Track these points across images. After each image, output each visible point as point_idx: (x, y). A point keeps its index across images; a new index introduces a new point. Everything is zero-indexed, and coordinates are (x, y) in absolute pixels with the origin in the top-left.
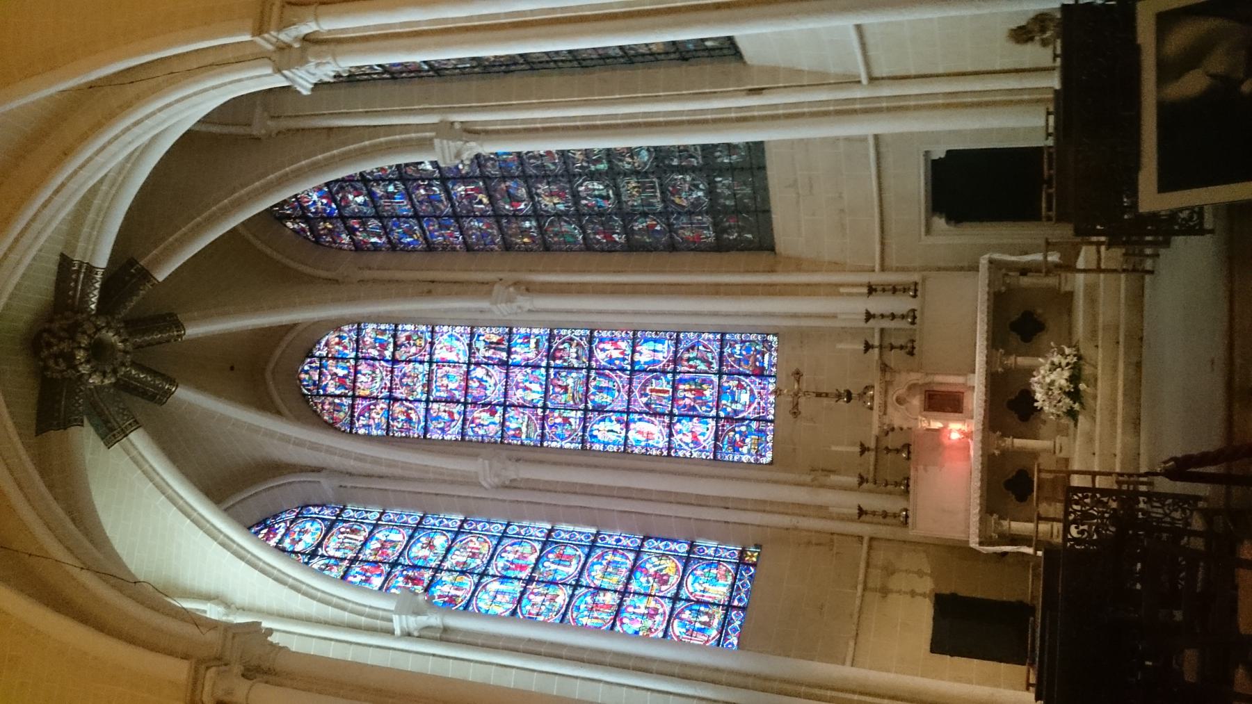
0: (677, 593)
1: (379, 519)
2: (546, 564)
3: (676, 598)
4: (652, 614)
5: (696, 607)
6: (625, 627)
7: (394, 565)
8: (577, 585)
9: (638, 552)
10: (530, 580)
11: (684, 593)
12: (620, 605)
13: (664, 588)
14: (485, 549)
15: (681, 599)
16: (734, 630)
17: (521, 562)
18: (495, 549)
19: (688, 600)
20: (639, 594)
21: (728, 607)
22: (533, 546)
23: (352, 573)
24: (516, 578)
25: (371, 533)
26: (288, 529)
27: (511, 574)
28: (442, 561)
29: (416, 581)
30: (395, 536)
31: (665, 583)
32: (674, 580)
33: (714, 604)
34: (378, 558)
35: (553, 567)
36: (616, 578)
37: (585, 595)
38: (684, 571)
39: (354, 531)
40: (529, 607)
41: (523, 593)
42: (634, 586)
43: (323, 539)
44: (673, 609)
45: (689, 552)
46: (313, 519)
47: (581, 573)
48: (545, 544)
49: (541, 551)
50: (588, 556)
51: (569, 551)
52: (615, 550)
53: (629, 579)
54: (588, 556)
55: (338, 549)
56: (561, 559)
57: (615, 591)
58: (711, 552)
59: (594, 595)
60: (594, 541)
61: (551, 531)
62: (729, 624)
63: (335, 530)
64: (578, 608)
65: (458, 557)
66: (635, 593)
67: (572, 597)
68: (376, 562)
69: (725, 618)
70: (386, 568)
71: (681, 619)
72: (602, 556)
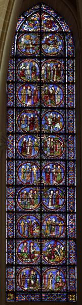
0: (44, 265)
1: (69, 83)
2: (52, 192)
3: (41, 265)
4: (31, 256)
5: (38, 277)
6: (22, 245)
7: (41, 108)
8: (41, 213)
9: (66, 239)
10: (41, 186)
11: (45, 269)
12: (34, 239)
13: (46, 258)
14: (57, 154)
15: (41, 268)
16: (29, 298)
17: (51, 177)
18: (57, 160)
19: (41, 271)
20: (41, 246)
21: (40, 292)
22: (62, 180)
23: (32, 87)
24: (41, 178)
25: (60, 83)
26: (55, 32)
27: (43, 175)
28: (46, 134)
29: (32, 125)
30: (58, 100)
31: (50, 258)
32: (52, 262)
33: (41, 285)
34: (43, 97)
35: (50, 196)
36: (49, 232)
37: (36, 219)
38: (58, 266)
39: (59, 73)
40: (25, 192)
41: (33, 186)
42: (46, 243)
43: (51, 58)
44: (35, 266)
45: (70, 265)
46: (64, 44)
47: (49, 212)
48: (64, 186)
49: (60, 186)
50: (60, 213)
51: (61, 202)
52: (65, 226)
53: (50, 239)
54: (60, 213)
55: (46, 70)
56: (56, 199)
57: (41, 234)
58: (72, 276)
59: (37, 223)
60: (70, 213)
61: (73, 186)
62: (32, 295)
63: (58, 61)
64: (29, 218)
65: (49, 141)
66: (41, 244)
67: (34, 212)
68: (40, 97)
69: (35, 292)
70: (38, 104)
71: (30, 271)
72: (60, 220)
